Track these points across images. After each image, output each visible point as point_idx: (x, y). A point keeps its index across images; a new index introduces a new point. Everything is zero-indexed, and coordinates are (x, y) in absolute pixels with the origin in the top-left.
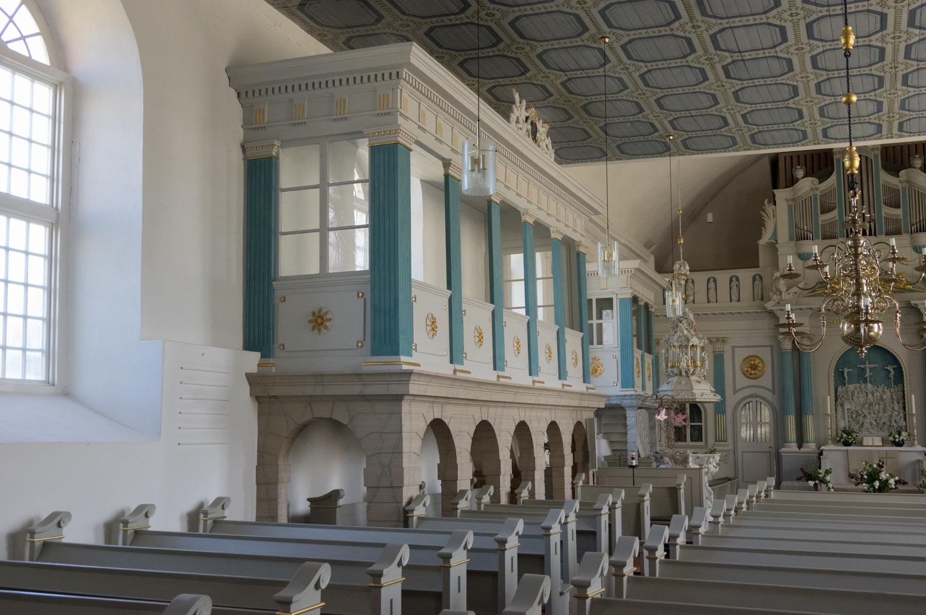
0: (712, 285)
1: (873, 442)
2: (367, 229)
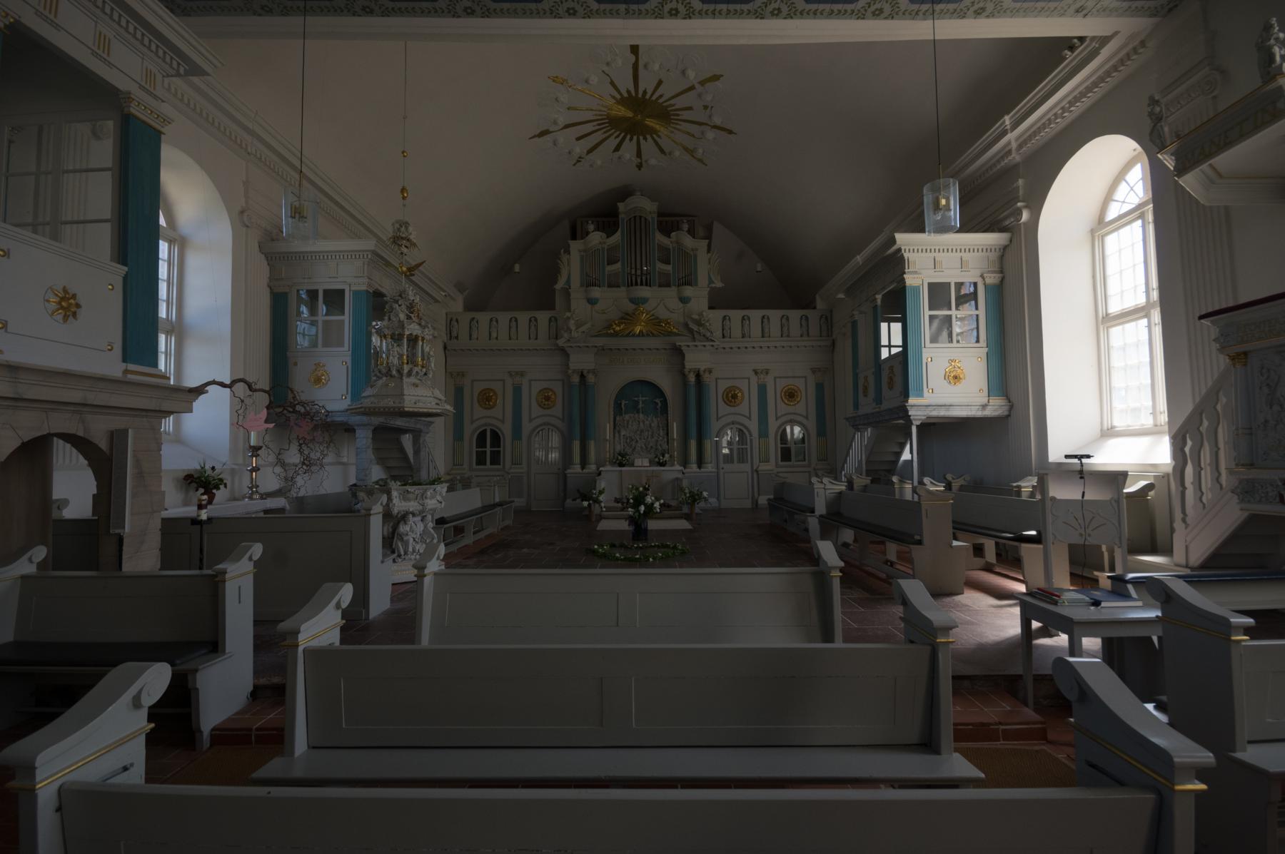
0: (514, 323)
1: (642, 463)
2: (108, 226)
